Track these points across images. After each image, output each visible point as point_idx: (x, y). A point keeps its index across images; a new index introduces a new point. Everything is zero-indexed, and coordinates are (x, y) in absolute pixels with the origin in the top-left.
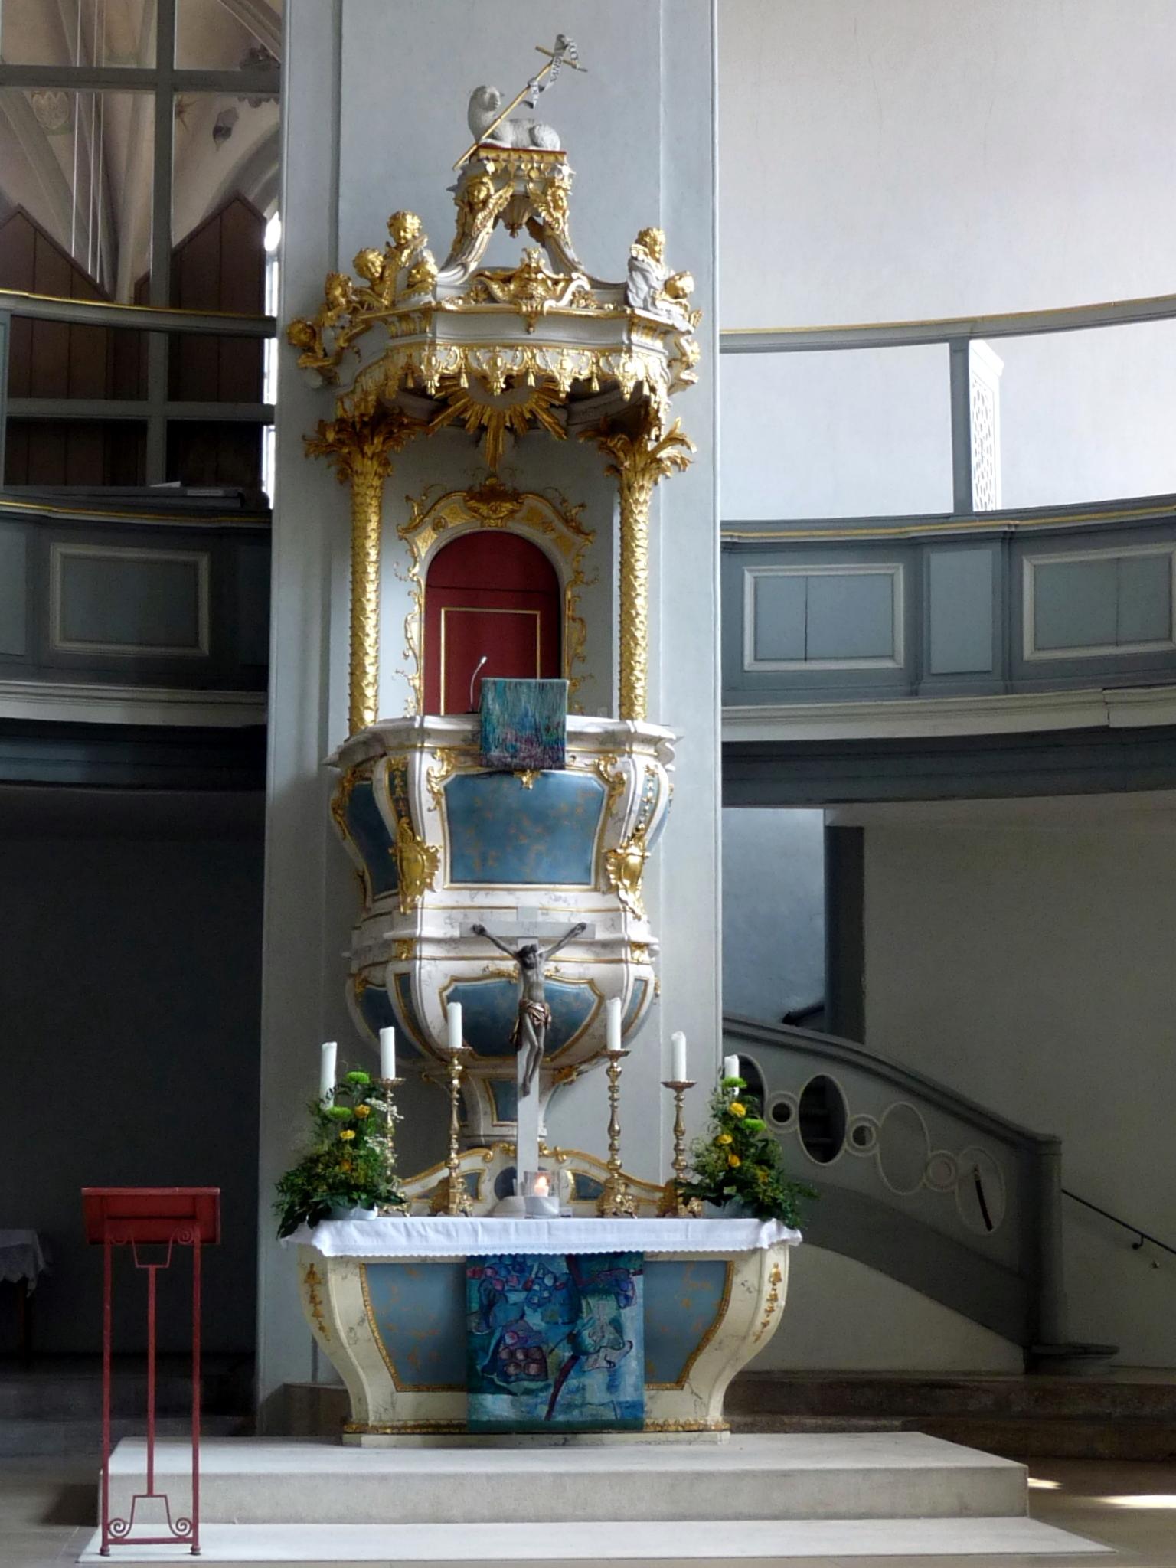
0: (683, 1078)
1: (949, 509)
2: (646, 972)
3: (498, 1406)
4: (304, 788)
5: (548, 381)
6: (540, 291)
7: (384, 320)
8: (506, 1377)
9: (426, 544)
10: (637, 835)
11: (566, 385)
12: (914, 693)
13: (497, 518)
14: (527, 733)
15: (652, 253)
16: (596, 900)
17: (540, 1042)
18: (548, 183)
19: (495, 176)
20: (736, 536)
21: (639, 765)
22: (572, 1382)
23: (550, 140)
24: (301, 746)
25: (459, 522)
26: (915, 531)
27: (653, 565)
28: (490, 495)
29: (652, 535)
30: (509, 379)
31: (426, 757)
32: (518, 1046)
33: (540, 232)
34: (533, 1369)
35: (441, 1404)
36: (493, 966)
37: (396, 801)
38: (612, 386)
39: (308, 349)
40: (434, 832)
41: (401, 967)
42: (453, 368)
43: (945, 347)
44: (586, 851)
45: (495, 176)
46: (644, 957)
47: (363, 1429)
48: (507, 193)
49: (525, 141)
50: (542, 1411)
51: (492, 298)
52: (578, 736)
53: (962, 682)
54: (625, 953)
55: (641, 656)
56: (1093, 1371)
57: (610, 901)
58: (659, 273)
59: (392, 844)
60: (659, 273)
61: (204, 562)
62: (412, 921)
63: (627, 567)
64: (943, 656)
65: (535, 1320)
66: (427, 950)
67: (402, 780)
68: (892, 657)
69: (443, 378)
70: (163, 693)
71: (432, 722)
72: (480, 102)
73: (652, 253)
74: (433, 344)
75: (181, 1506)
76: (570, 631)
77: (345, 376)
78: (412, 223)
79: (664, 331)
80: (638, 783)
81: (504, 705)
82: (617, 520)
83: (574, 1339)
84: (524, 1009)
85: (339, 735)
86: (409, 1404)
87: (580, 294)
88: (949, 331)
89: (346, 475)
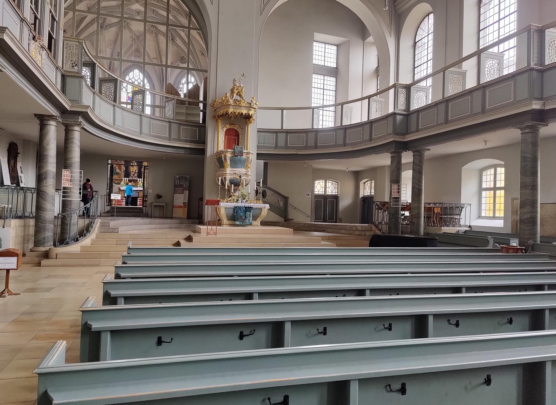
2: (250, 178)
3: (238, 223)
4: (211, 156)
5: (242, 114)
6: (242, 103)
7: (224, 105)
8: (238, 220)
9: (225, 129)
11: (244, 114)
13: (232, 127)
14: (239, 152)
15: (254, 100)
18: (241, 90)
19: (236, 89)
22: (245, 221)
23: (242, 85)
24: (211, 151)
25: (228, 127)
26: (277, 131)
28: (232, 124)
30: (238, 113)
33: (240, 96)
34: (241, 219)
35: (231, 222)
38: (249, 114)
39: (213, 106)
41: (225, 176)
42: (232, 111)
45: (236, 89)
47: (223, 225)
48: (237, 91)
49: (239, 86)
50: (242, 223)
51: (236, 104)
53: (281, 147)
54: (248, 176)
55: (249, 144)
56: (291, 221)
57: (247, 170)
58: (254, 102)
60: (254, 102)
61: (198, 129)
63: (247, 133)
65: (241, 214)
67: (225, 156)
68: (273, 144)
69: (231, 112)
70: (194, 144)
71: (229, 150)
72: (234, 80)
73: (254, 100)
74: (230, 108)
75: (215, 231)
76: (240, 140)
77: (217, 110)
78: (228, 94)
79: (255, 108)
81: (237, 149)
82: (246, 128)
83: (245, 216)
84: (240, 182)
85: (215, 150)
86: (228, 222)
87: (246, 104)
88: (281, 109)
89: (217, 121)
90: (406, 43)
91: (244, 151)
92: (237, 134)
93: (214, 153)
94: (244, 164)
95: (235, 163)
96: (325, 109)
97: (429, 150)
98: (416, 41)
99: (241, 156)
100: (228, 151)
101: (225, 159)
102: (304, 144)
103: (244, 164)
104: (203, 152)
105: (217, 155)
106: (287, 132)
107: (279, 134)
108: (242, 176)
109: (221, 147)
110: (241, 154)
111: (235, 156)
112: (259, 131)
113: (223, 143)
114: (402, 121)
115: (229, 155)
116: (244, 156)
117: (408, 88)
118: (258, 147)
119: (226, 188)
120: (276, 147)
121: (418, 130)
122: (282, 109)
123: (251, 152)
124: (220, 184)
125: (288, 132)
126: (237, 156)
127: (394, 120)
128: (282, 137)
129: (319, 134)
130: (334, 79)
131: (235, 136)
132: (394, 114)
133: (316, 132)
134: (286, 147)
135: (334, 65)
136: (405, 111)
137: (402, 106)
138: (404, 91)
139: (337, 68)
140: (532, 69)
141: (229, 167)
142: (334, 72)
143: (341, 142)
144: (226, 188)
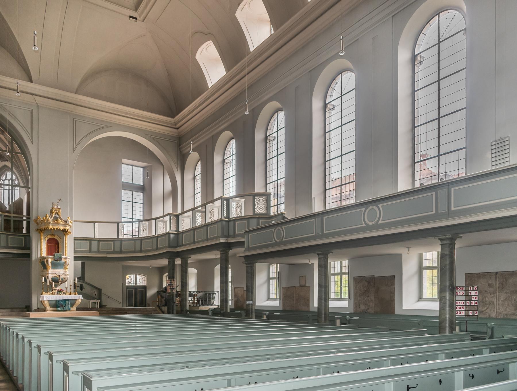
0: (71, 285)
1: (93, 237)
4: (36, 260)
10: (67, 266)
12: (90, 253)
16: (64, 271)
17: (61, 282)
20: (76, 238)
21: (68, 260)
24: (36, 256)
27: (68, 242)
29: (68, 240)
31: (50, 259)
32: (59, 283)
36: (55, 276)
37: (47, 262)
40: (50, 265)
41: (47, 276)
43: (93, 223)
44: (63, 267)
46: (68, 275)
52: (63, 258)
59: (46, 265)
62: (48, 272)
64: (93, 250)
66: (50, 274)
67: (47, 261)
71: (50, 256)
76: (60, 247)
80: (68, 262)
81: (57, 255)
84: (59, 280)
85: (39, 256)
90: (188, 177)
91: (62, 257)
92: (57, 243)
93: (39, 257)
94: (63, 266)
95: (55, 265)
96: (131, 220)
97: (190, 257)
98: (195, 175)
99: (60, 261)
100: (49, 257)
101: (47, 263)
102: (112, 250)
103: (63, 266)
104: (29, 256)
105: (41, 259)
106: (98, 240)
107: (92, 242)
108: (61, 275)
109: (44, 254)
110: (60, 259)
111: (55, 261)
112: (76, 239)
113: (46, 250)
114: (174, 238)
115: (50, 260)
116: (63, 261)
117: (177, 216)
118: (75, 251)
119: (48, 284)
120: (90, 251)
121: (183, 245)
122: (94, 223)
123: (68, 257)
124: (43, 282)
125: (99, 240)
126: (57, 261)
127: (169, 236)
128: (94, 243)
129: (123, 242)
130: (141, 194)
131: (56, 244)
132: (168, 234)
133: (121, 240)
134: (98, 252)
135: (141, 184)
136: (176, 231)
137: (174, 228)
138: (175, 218)
139: (143, 186)
140: (222, 221)
141: (51, 268)
142: (142, 189)
143: (138, 249)
144: (48, 284)
